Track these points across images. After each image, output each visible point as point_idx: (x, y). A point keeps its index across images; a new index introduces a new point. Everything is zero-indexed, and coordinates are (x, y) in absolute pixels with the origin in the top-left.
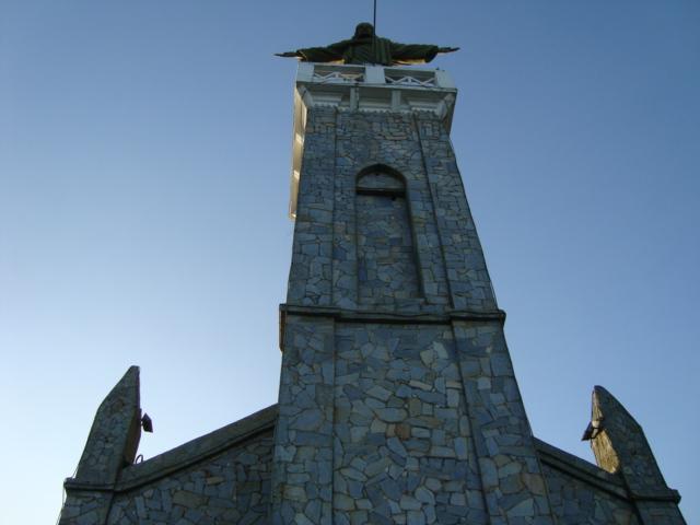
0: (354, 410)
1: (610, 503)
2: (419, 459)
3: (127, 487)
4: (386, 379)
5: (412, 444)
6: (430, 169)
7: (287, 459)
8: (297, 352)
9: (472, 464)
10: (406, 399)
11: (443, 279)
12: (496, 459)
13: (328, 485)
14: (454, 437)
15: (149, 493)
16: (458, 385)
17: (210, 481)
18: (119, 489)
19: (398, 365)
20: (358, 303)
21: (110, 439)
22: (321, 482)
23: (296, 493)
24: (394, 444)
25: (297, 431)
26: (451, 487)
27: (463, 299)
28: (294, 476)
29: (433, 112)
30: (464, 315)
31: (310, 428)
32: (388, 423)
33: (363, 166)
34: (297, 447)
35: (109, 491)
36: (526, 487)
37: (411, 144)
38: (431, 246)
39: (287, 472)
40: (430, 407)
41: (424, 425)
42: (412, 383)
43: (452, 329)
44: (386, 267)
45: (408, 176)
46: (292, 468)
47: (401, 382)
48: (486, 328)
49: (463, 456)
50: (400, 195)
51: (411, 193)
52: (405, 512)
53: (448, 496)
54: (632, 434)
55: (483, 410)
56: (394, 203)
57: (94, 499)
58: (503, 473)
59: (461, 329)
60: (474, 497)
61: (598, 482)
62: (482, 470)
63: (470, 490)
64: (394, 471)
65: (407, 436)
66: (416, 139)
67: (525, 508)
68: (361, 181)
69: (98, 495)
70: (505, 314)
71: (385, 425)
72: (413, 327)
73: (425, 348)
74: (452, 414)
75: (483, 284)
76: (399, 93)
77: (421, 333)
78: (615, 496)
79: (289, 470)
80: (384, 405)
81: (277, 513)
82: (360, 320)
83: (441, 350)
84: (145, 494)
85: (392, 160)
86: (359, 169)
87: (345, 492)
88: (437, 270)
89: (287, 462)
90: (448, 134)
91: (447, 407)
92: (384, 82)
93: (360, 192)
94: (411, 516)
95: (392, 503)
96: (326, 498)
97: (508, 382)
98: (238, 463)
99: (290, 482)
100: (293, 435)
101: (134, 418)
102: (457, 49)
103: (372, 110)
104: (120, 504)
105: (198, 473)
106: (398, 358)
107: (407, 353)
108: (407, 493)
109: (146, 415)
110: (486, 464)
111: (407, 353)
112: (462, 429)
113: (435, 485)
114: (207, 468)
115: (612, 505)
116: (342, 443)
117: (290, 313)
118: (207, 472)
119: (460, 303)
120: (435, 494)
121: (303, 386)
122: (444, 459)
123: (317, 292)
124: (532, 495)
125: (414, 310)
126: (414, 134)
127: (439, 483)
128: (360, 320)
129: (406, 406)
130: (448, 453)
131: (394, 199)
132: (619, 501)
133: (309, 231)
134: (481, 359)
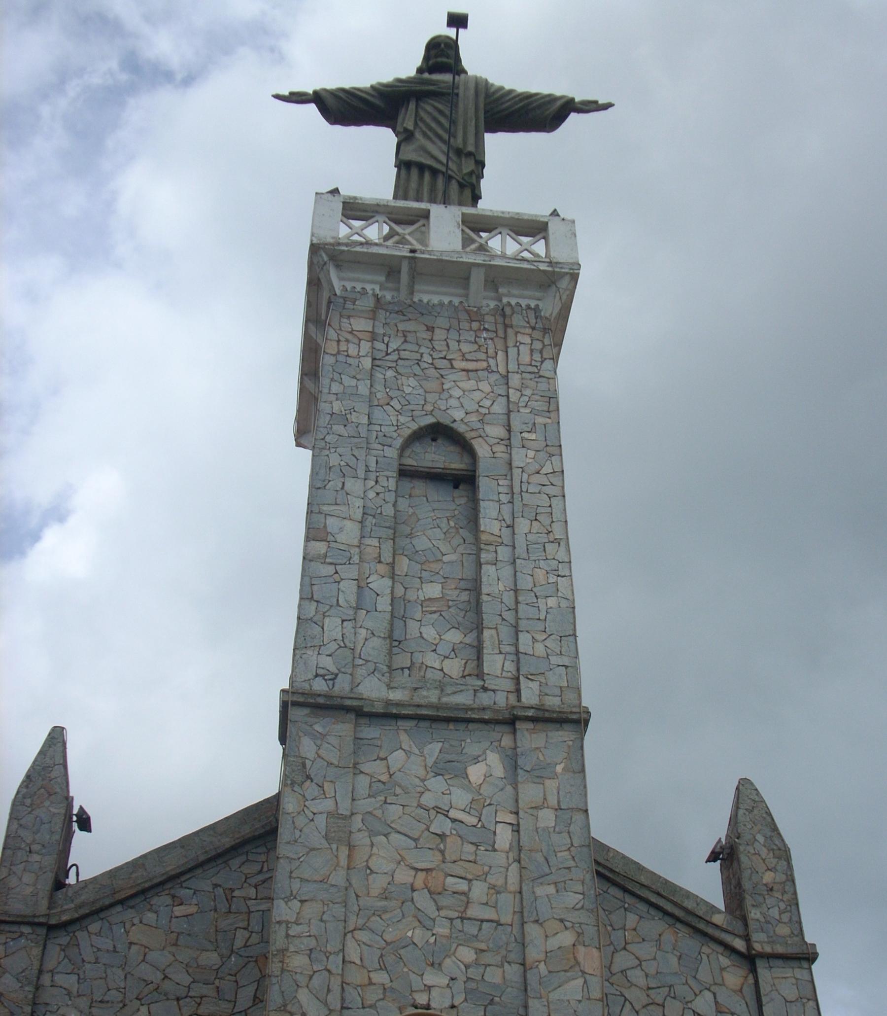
0: (375, 850)
1: (721, 958)
2: (451, 920)
3: (65, 918)
4: (420, 806)
5: (444, 901)
6: (516, 441)
7: (288, 918)
8: (304, 765)
9: (516, 930)
10: (442, 836)
11: (512, 649)
12: (546, 925)
13: (336, 953)
14: (498, 892)
15: (94, 927)
16: (511, 818)
17: (179, 911)
18: (53, 921)
19: (437, 784)
20: (389, 687)
21: (35, 847)
22: (329, 949)
23: (298, 962)
24: (423, 900)
25: (302, 880)
26: (488, 958)
27: (535, 686)
28: (297, 941)
29: (536, 309)
30: (530, 713)
31: (318, 877)
32: (417, 870)
33: (414, 426)
34: (302, 902)
35: (40, 924)
36: (578, 963)
37: (494, 377)
38: (501, 588)
39: (288, 936)
40: (472, 848)
41: (463, 875)
42: (453, 814)
43: (514, 732)
44: (435, 616)
45: (482, 449)
46: (294, 930)
47: (438, 810)
48: (560, 733)
49: (506, 918)
50: (464, 481)
51: (484, 484)
52: (429, 988)
53: (481, 970)
54: (774, 861)
55: (539, 857)
56: (457, 493)
57: (22, 934)
58: (554, 943)
59: (526, 734)
60: (513, 972)
61: (710, 930)
62: (527, 940)
63: (509, 962)
64: (418, 935)
65: (440, 890)
66: (502, 369)
67: (573, 988)
68: (408, 452)
69: (26, 930)
70: (589, 713)
71: (413, 873)
72: (462, 726)
73: (476, 760)
74: (500, 859)
75: (566, 661)
76: (482, 271)
77: (473, 742)
78: (733, 950)
79: (291, 933)
80: (413, 844)
81: (276, 987)
82: (389, 715)
83: (494, 762)
84: (90, 928)
85: (458, 415)
86: (407, 432)
87: (358, 962)
88: (505, 632)
89: (287, 922)
90: (555, 359)
91: (495, 850)
92: (458, 246)
93: (405, 473)
94: (435, 993)
95: (412, 976)
96: (334, 971)
97: (578, 817)
98: (216, 886)
99: (292, 949)
100: (296, 885)
101: (65, 815)
102: (607, 106)
103: (435, 300)
104: (58, 941)
105: (161, 900)
106: (438, 774)
107: (451, 768)
108: (432, 965)
109: (81, 808)
110: (532, 930)
111: (451, 768)
112: (510, 881)
113: (467, 954)
114: (172, 892)
115: (725, 961)
116: (357, 896)
117: (295, 704)
118: (173, 897)
119: (530, 694)
120: (467, 967)
121: (311, 816)
122: (482, 921)
123: (333, 669)
124: (583, 972)
125: (463, 699)
126: (501, 355)
127: (473, 952)
128: (389, 715)
129: (442, 846)
130: (489, 914)
131: (456, 487)
132: (734, 956)
133: (323, 559)
134: (548, 782)
